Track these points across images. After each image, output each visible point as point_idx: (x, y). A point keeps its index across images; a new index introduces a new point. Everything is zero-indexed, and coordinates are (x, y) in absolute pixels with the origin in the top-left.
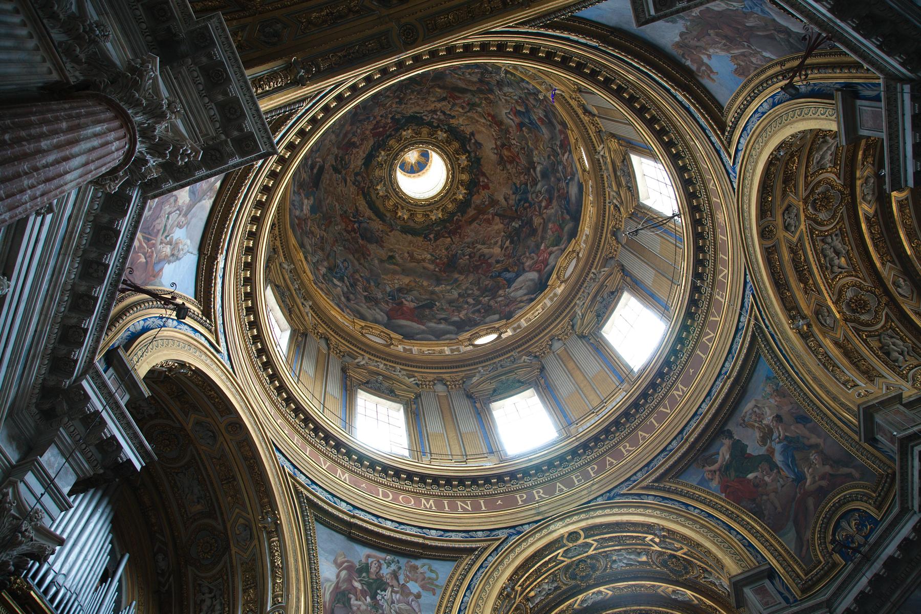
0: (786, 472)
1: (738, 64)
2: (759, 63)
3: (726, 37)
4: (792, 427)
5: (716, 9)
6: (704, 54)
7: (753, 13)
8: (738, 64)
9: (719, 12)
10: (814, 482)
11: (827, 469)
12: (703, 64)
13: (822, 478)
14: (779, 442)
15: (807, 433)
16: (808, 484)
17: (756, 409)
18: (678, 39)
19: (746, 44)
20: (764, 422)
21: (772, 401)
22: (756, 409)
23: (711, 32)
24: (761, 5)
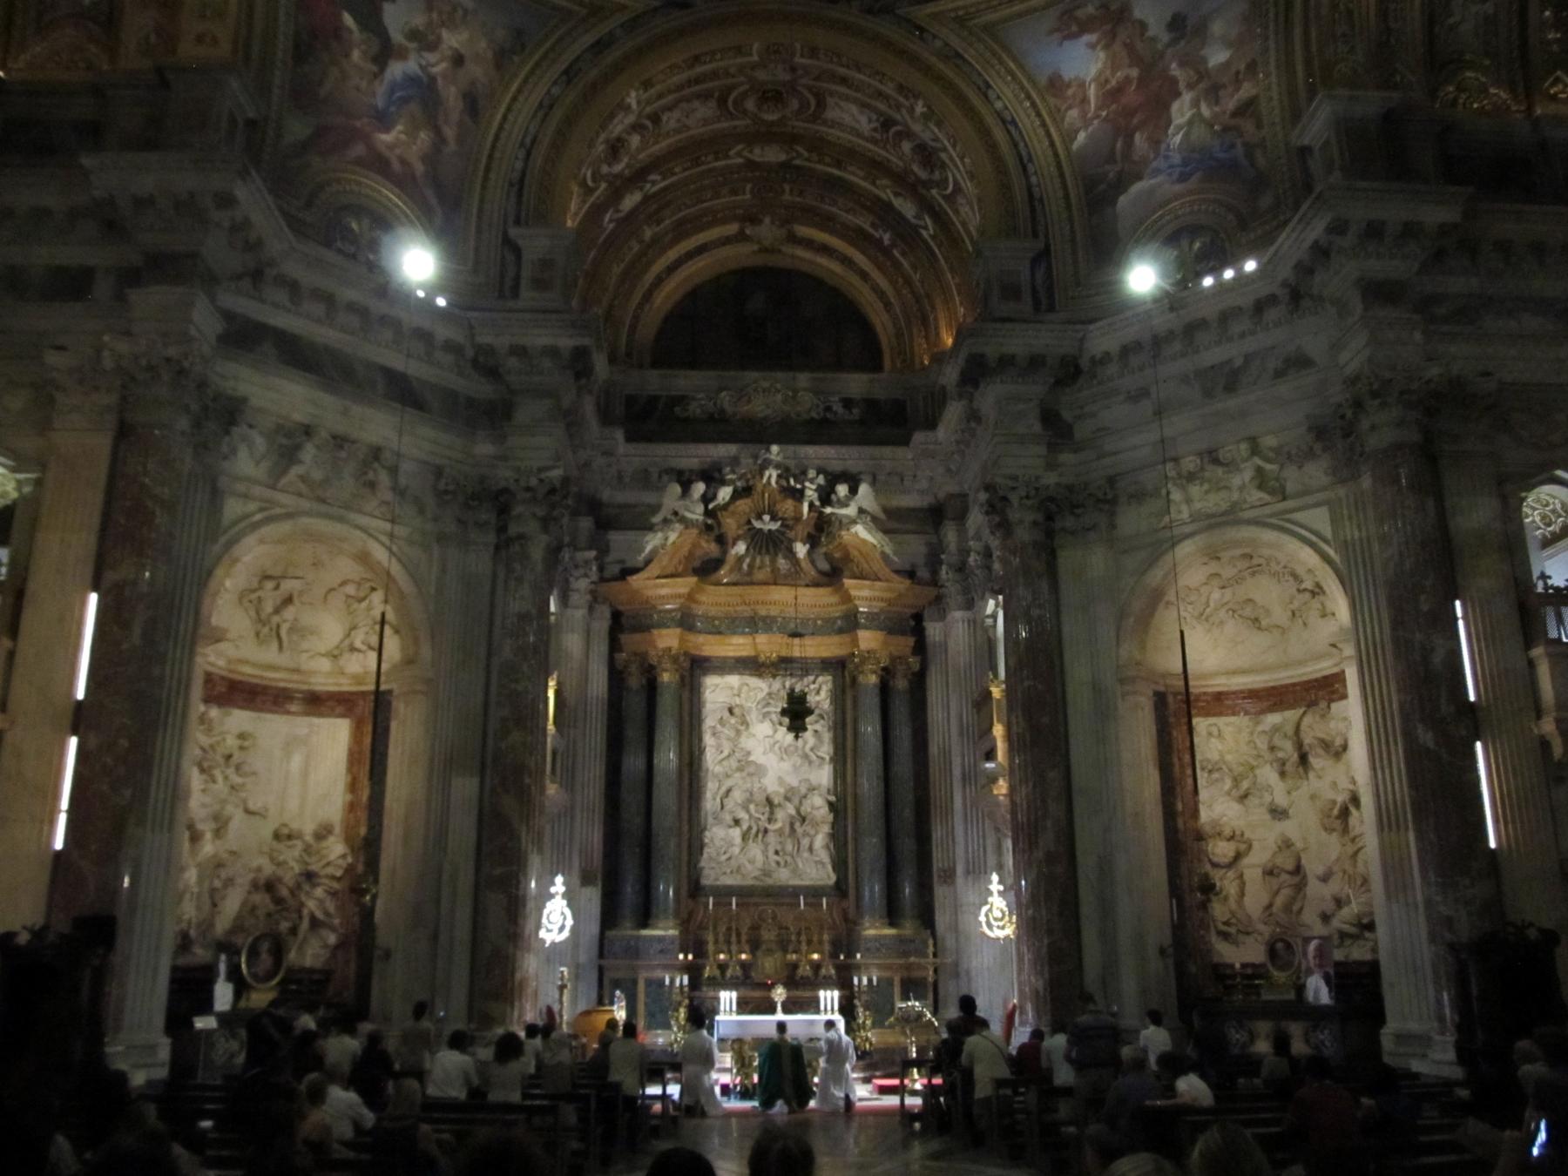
0: (381, 89)
1: (1069, 86)
2: (1067, 119)
3: (1119, 90)
4: (453, 89)
5: (1175, 106)
6: (1098, 42)
7: (1157, 155)
8: (1069, 86)
9: (1166, 107)
10: (391, 147)
11: (419, 168)
12: (1084, 27)
13: (403, 162)
14: (421, 66)
15: (455, 116)
16: (387, 137)
17: (460, 12)
18: (1138, 14)
19: (1104, 114)
20: (445, 34)
21: (483, 44)
22: (460, 12)
23: (1134, 73)
24: (1170, 174)
